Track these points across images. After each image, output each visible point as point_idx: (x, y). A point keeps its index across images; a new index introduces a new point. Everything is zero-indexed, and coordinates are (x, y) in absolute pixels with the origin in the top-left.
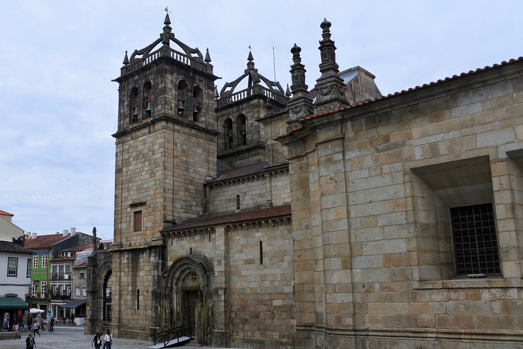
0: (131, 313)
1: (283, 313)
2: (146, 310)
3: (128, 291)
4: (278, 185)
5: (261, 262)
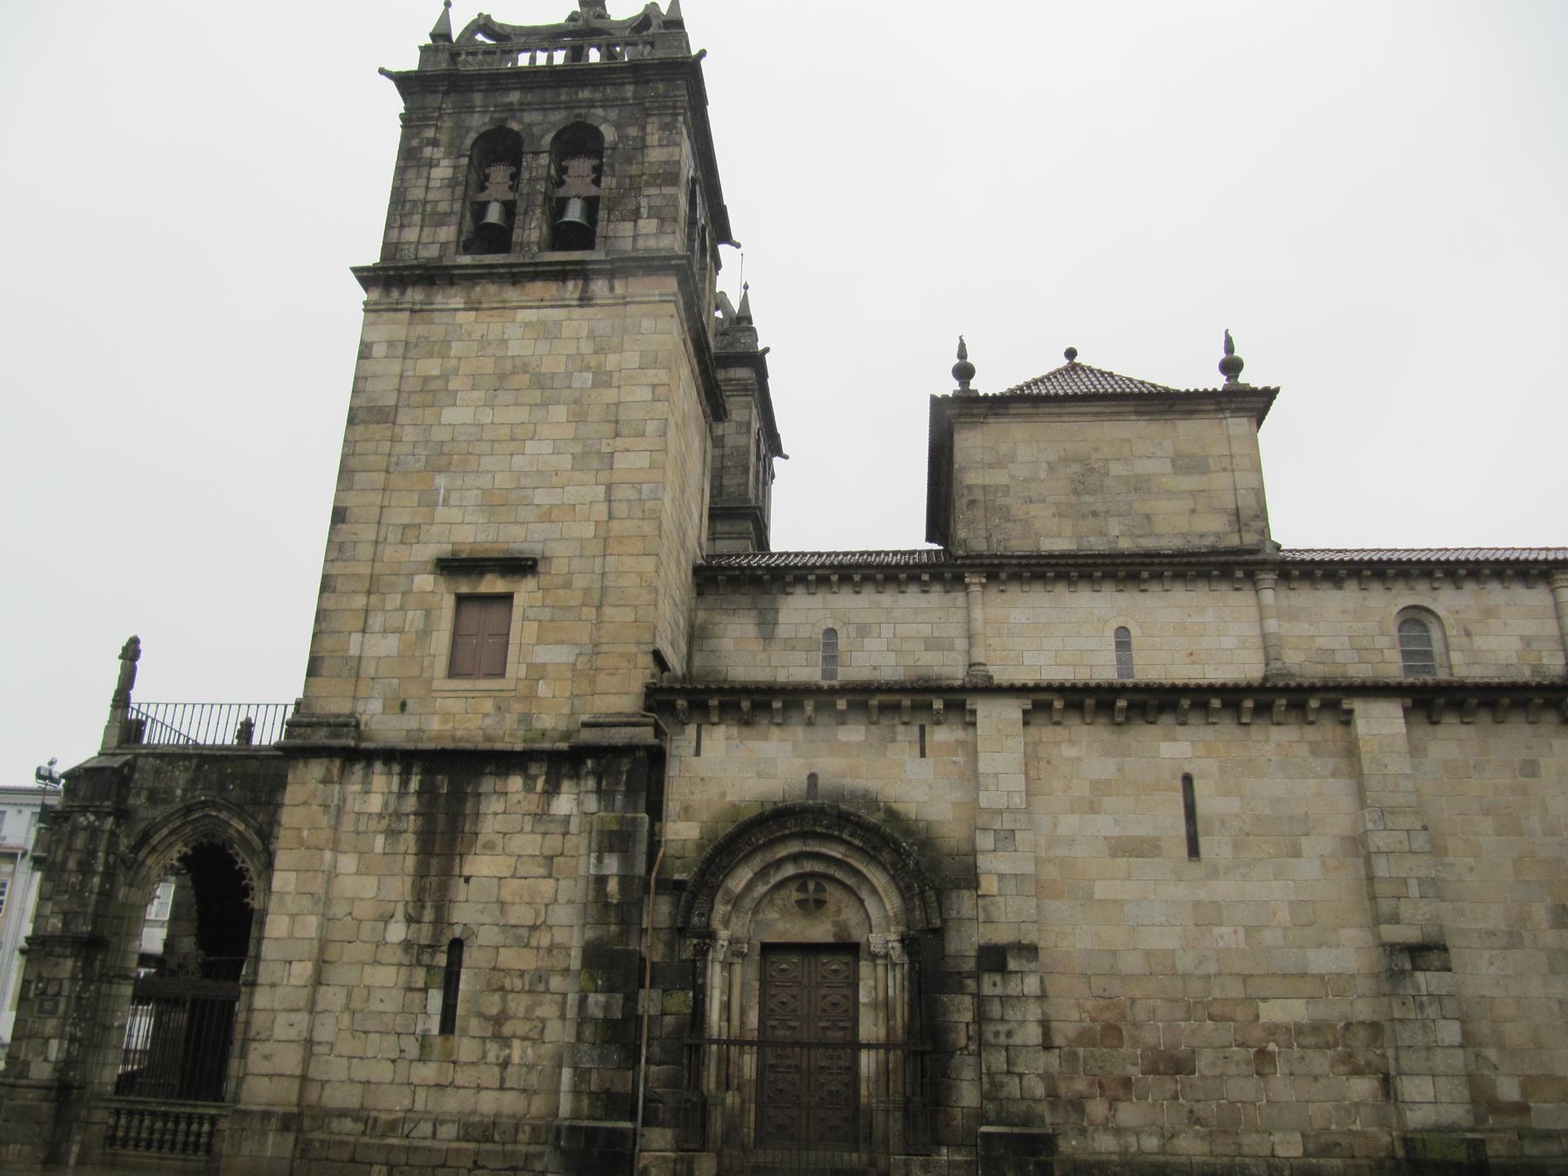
0: (394, 1055)
1: (1311, 1054)
2: (505, 1041)
3: (381, 943)
4: (1012, 621)
5: (1194, 851)
